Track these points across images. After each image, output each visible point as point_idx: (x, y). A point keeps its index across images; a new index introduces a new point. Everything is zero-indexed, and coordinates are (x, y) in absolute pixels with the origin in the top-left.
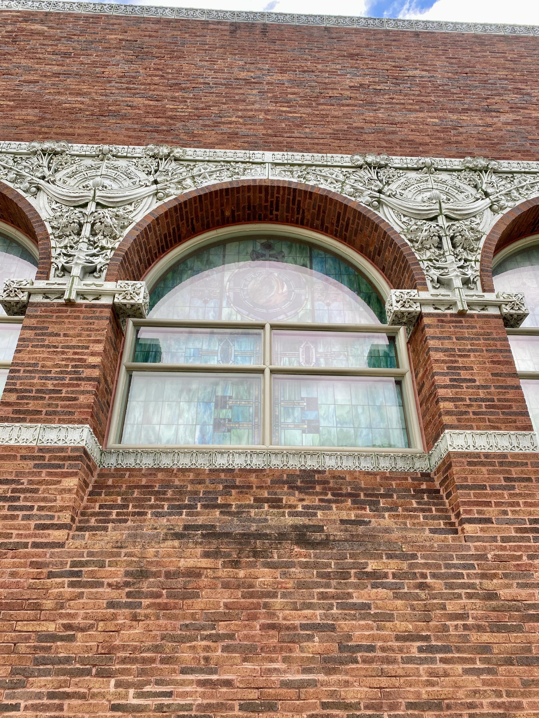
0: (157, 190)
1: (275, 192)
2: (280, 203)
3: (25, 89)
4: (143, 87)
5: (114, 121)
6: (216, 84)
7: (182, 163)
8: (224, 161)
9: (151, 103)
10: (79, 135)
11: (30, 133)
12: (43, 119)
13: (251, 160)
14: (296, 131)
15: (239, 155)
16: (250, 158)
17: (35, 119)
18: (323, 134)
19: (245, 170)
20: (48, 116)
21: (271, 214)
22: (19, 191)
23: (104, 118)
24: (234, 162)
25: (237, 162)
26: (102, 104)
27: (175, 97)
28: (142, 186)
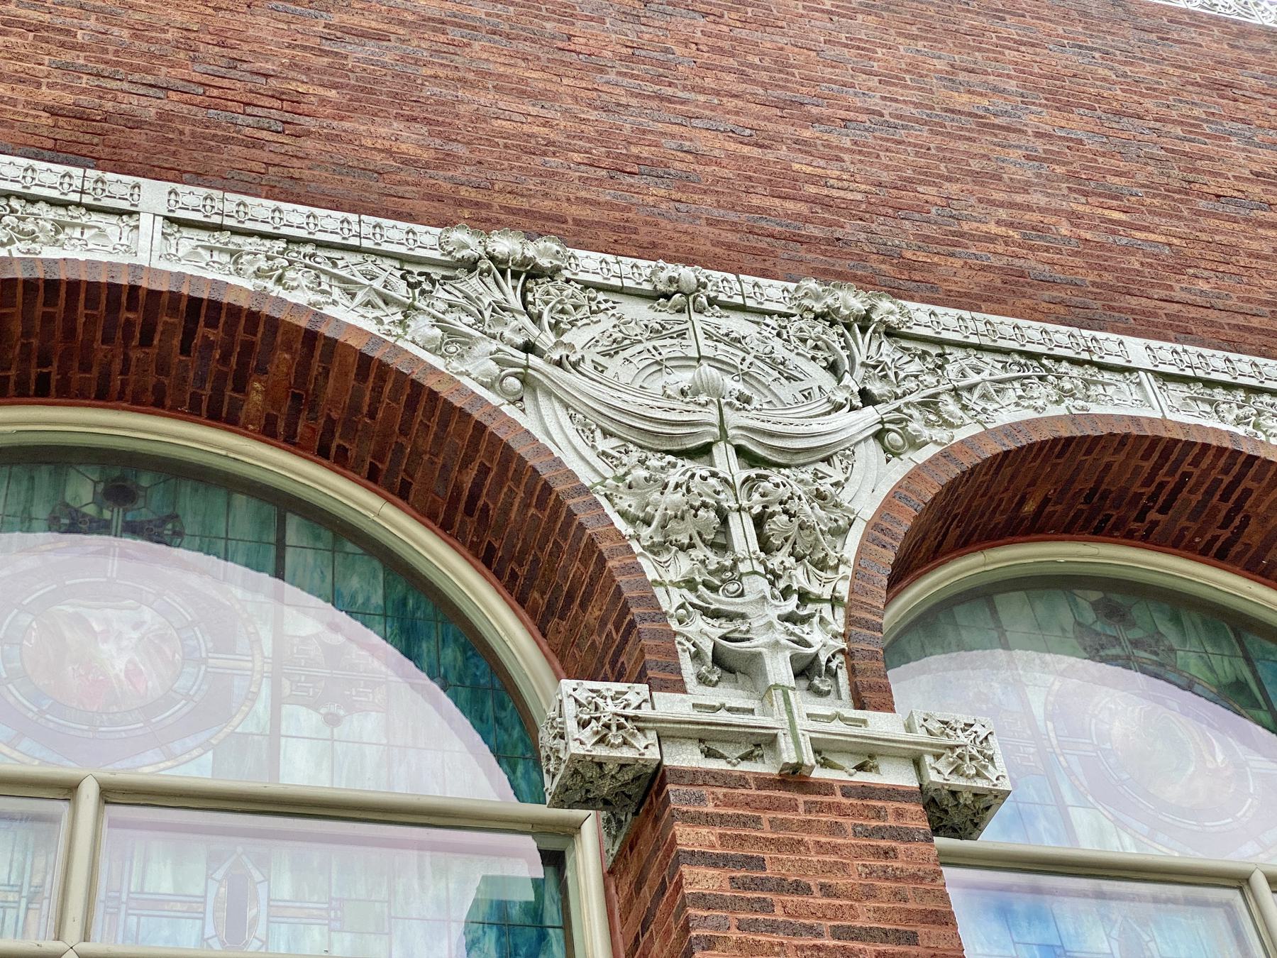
0: (882, 422)
1: (1189, 459)
2: (1185, 490)
3: (357, 52)
4: (702, 98)
5: (662, 192)
6: (900, 117)
7: (905, 344)
8: (1021, 353)
9: (746, 150)
10: (577, 222)
11: (429, 197)
12: (447, 160)
13: (1095, 358)
14: (1177, 286)
15: (115, 189)
16: (1089, 350)
17: (426, 156)
18: (1248, 300)
19: (1087, 383)
20: (461, 150)
21: (1141, 518)
22: (465, 381)
23: (629, 180)
24: (1049, 357)
25: (1058, 359)
26: (604, 137)
27: (805, 142)
28: (841, 406)
